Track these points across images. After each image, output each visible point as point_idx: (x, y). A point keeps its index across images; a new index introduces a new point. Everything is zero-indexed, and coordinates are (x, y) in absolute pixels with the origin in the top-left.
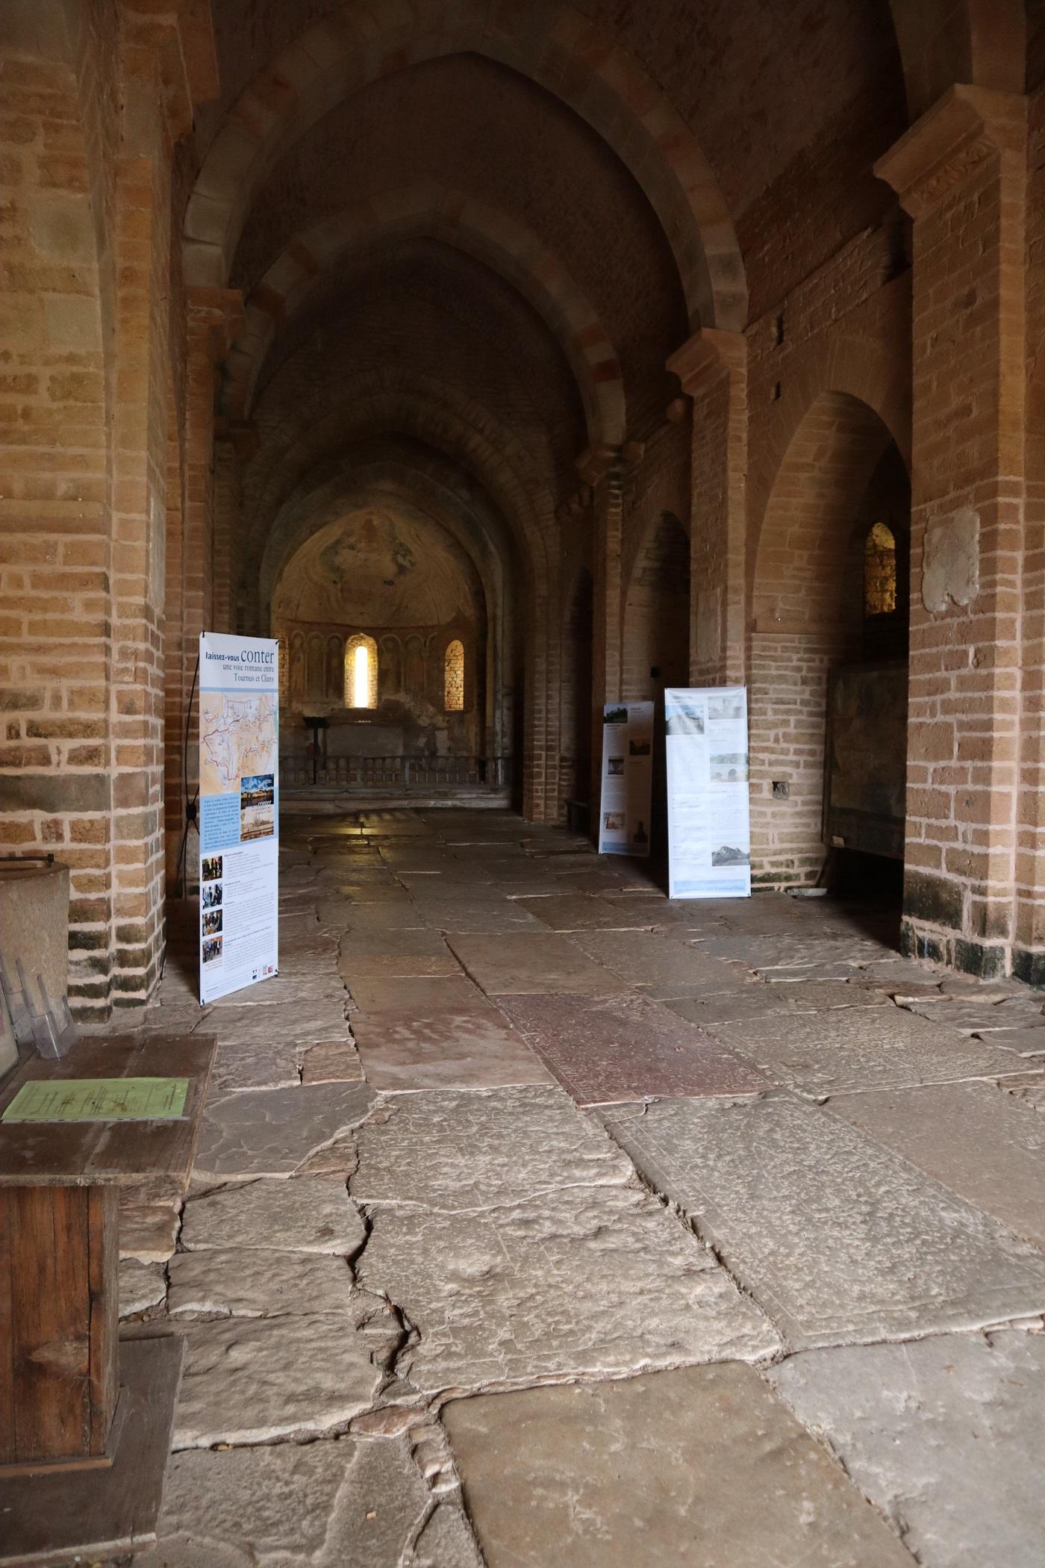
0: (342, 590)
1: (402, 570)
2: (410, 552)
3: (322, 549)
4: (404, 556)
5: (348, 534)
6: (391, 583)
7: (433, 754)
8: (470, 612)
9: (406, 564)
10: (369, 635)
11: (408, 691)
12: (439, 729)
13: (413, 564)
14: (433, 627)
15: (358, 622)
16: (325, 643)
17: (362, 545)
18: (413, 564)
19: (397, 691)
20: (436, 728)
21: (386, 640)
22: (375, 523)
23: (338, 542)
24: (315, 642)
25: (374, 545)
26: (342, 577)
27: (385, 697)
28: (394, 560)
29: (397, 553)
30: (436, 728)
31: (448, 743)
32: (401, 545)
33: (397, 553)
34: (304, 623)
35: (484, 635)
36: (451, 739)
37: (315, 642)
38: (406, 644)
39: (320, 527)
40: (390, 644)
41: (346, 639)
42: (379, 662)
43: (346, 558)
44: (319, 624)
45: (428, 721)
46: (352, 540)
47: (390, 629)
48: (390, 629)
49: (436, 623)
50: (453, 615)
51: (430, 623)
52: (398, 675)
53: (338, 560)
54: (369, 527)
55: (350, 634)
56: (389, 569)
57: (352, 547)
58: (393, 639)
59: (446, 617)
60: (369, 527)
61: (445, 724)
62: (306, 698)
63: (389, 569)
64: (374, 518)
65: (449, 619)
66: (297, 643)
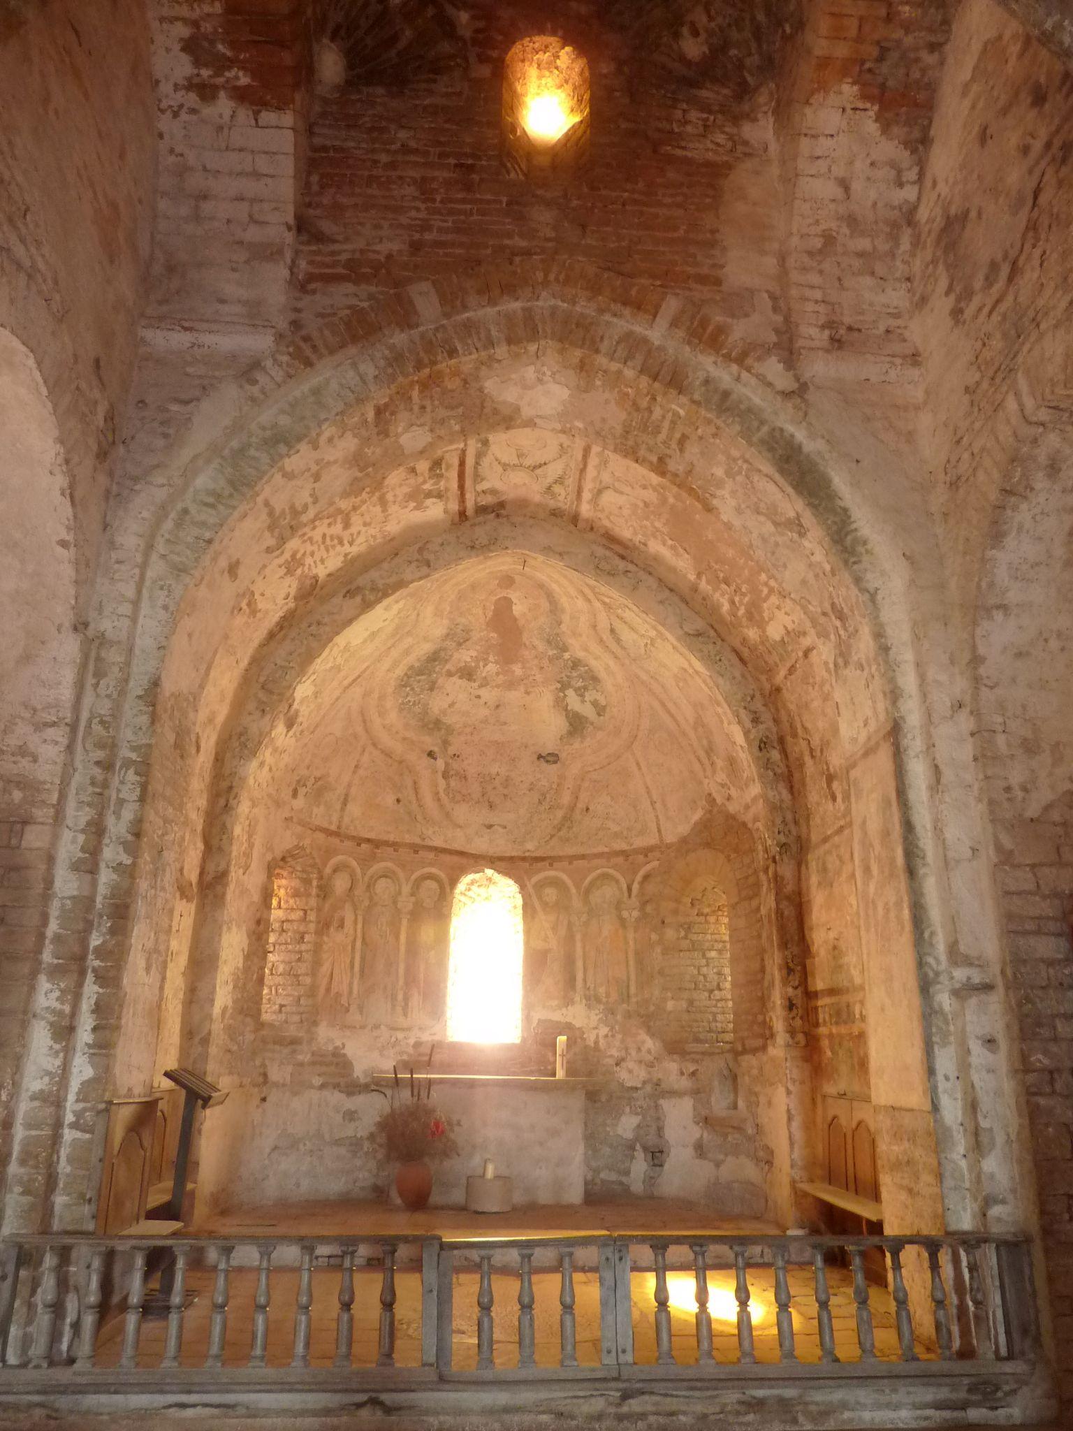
0: (446, 775)
1: (576, 725)
2: (595, 679)
3: (400, 671)
4: (581, 692)
5: (459, 637)
6: (551, 758)
7: (657, 1155)
8: (750, 796)
9: (587, 711)
10: (507, 873)
11: (592, 1000)
12: (673, 1093)
13: (600, 710)
14: (646, 851)
15: (480, 845)
16: (406, 889)
17: (492, 668)
18: (600, 710)
19: (568, 1002)
20: (660, 1091)
21: (540, 886)
22: (518, 609)
23: (435, 658)
24: (382, 884)
25: (517, 670)
26: (446, 743)
27: (540, 1014)
28: (560, 703)
29: (564, 686)
30: (660, 1091)
31: (696, 1132)
32: (576, 664)
33: (564, 686)
34: (360, 841)
35: (796, 848)
36: (706, 1121)
37: (382, 884)
38: (588, 892)
39: (383, 593)
40: (551, 893)
41: (454, 882)
42: (527, 932)
43: (454, 698)
44: (395, 845)
45: (642, 1073)
46: (466, 656)
47: (551, 860)
48: (551, 860)
49: (652, 840)
50: (697, 816)
51: (639, 842)
52: (569, 961)
53: (437, 704)
54: (503, 620)
55: (463, 871)
56: (548, 726)
57: (467, 673)
58: (555, 883)
59: (677, 828)
60: (503, 620)
61: (685, 1083)
62: (354, 1017)
63: (548, 726)
64: (514, 596)
65: (684, 829)
66: (340, 884)
